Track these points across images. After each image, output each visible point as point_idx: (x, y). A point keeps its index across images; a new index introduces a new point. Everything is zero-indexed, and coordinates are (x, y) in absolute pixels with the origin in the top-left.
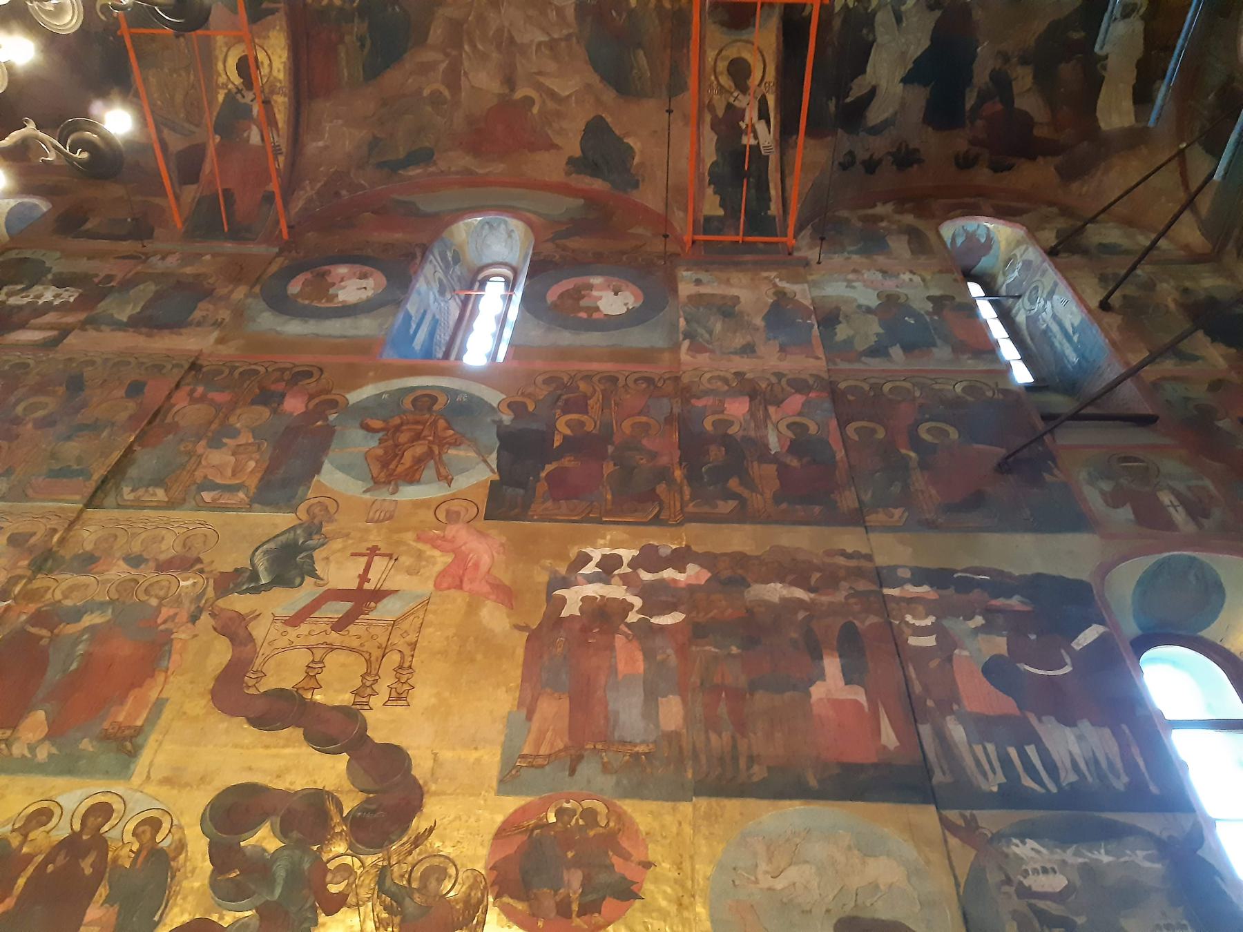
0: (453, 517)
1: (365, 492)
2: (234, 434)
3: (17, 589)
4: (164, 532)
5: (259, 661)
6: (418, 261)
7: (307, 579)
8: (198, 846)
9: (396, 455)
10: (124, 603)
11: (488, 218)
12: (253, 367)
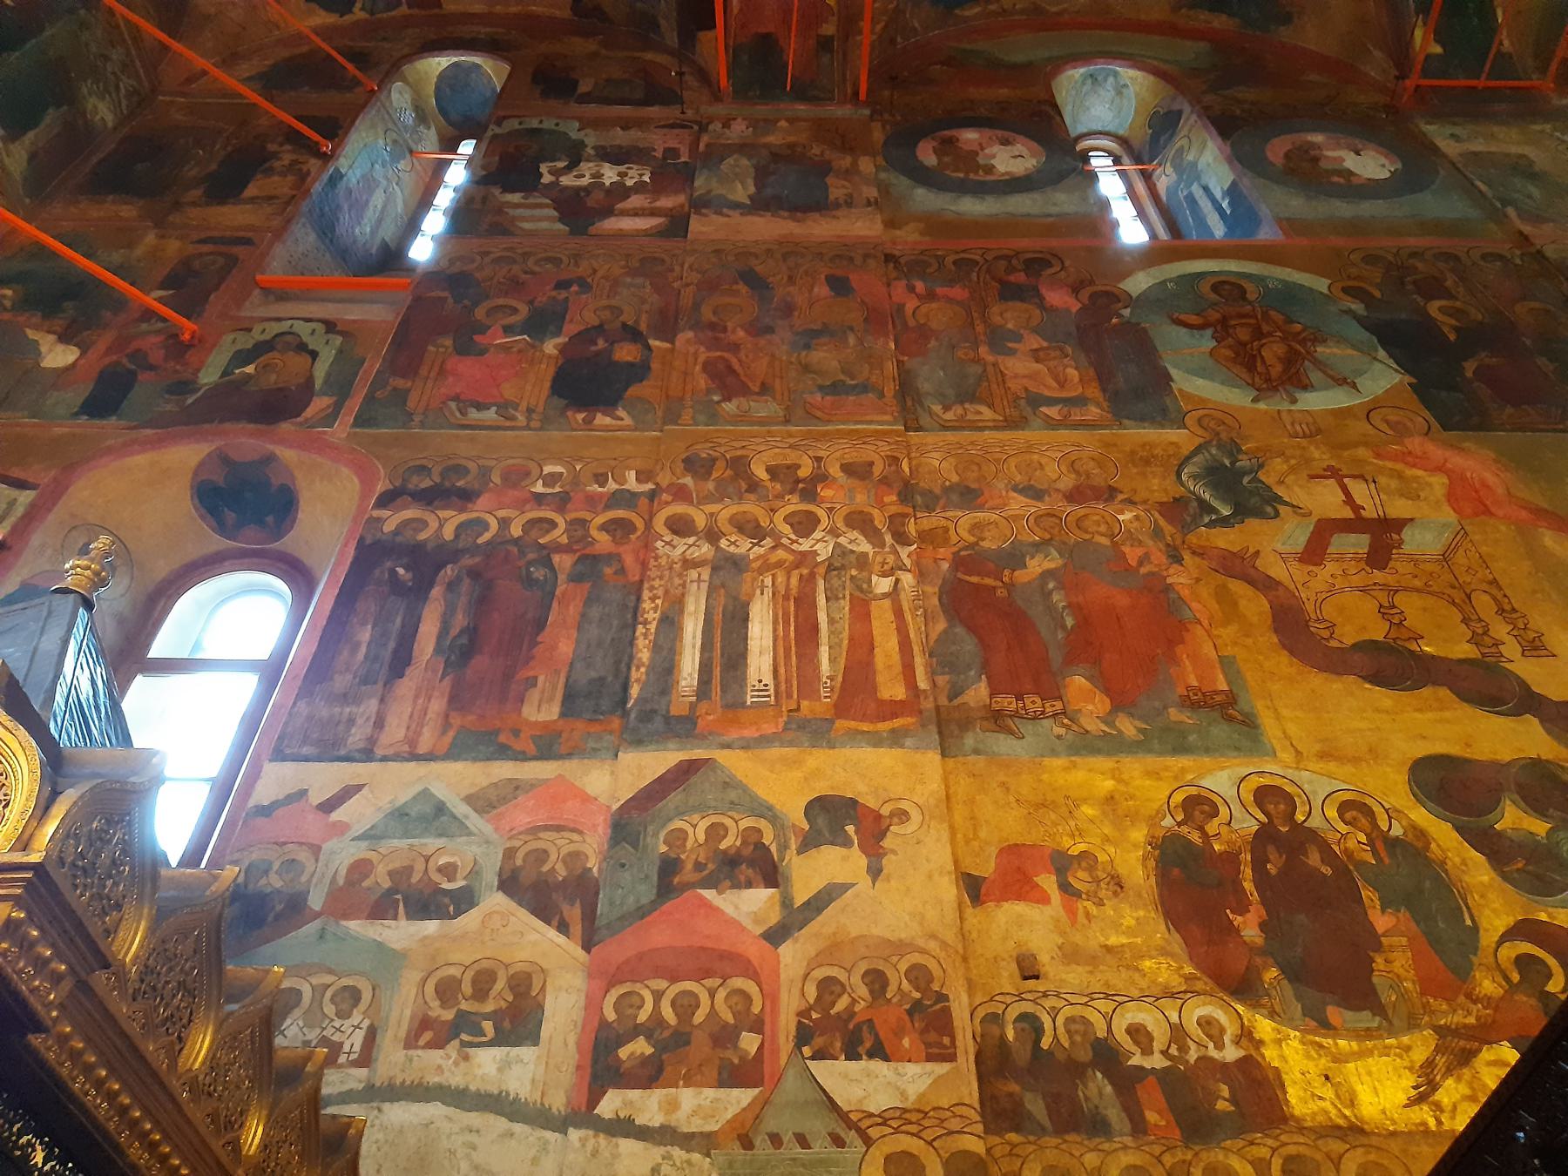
0: (1400, 431)
1: (1255, 400)
2: (1018, 338)
3: (912, 529)
4: (1036, 457)
5: (1310, 607)
6: (1058, 118)
7: (1282, 509)
8: (1444, 836)
9: (1255, 356)
10: (1064, 543)
11: (1097, 67)
12: (963, 255)
